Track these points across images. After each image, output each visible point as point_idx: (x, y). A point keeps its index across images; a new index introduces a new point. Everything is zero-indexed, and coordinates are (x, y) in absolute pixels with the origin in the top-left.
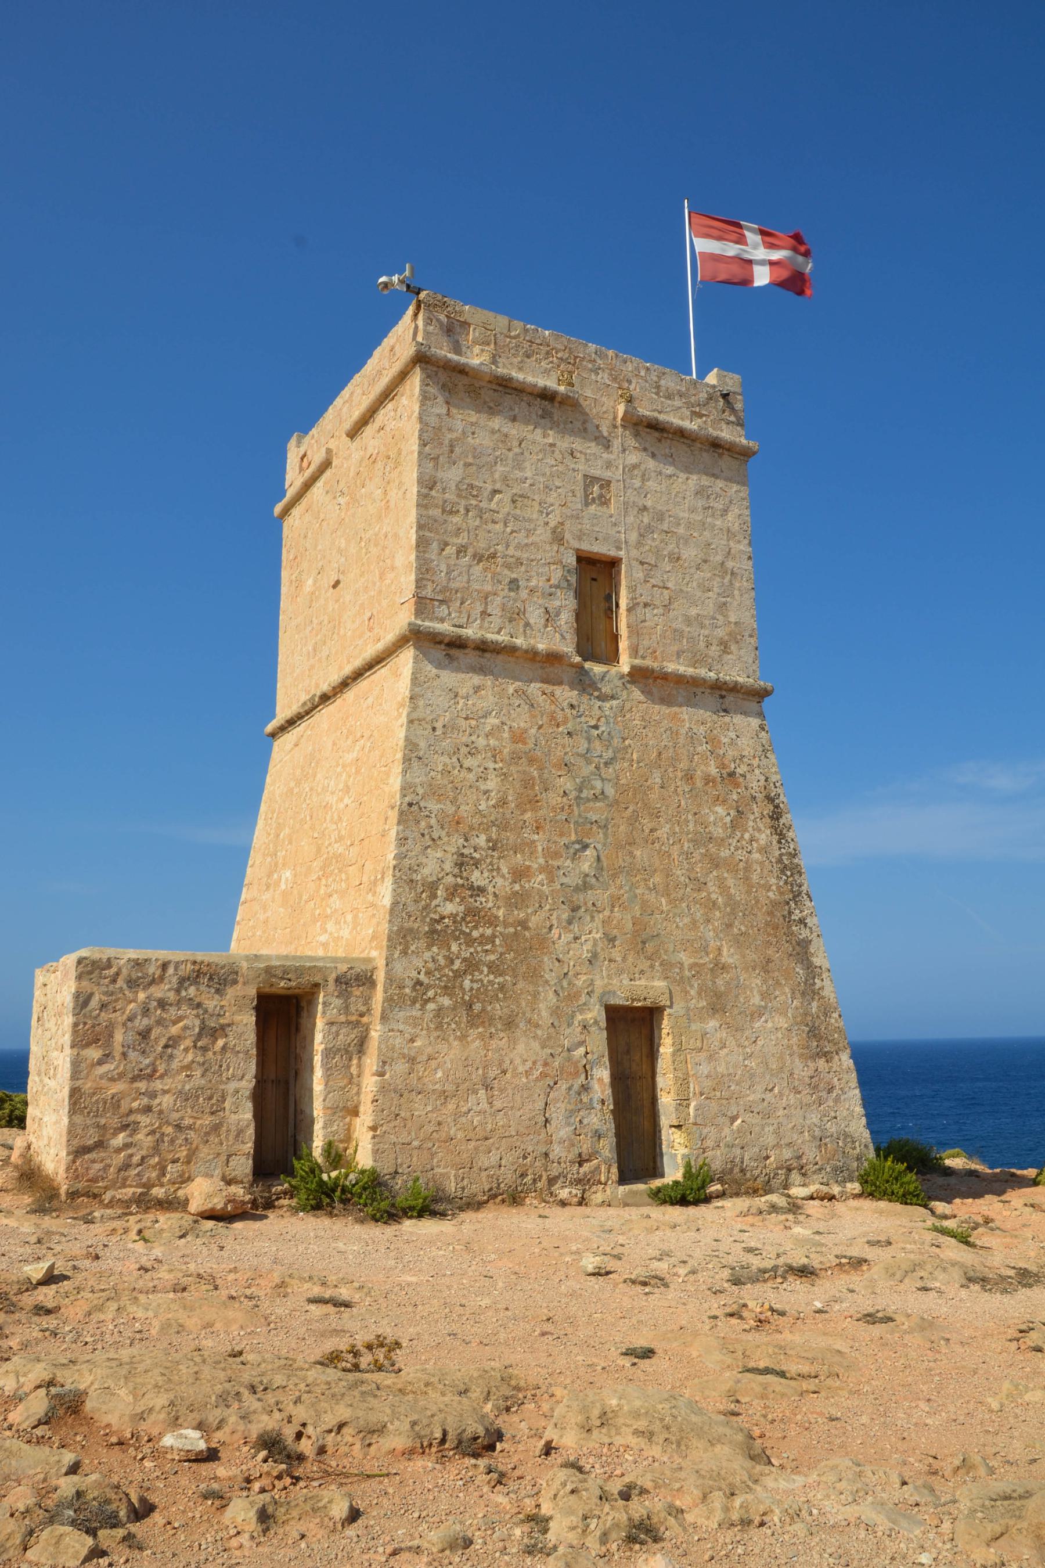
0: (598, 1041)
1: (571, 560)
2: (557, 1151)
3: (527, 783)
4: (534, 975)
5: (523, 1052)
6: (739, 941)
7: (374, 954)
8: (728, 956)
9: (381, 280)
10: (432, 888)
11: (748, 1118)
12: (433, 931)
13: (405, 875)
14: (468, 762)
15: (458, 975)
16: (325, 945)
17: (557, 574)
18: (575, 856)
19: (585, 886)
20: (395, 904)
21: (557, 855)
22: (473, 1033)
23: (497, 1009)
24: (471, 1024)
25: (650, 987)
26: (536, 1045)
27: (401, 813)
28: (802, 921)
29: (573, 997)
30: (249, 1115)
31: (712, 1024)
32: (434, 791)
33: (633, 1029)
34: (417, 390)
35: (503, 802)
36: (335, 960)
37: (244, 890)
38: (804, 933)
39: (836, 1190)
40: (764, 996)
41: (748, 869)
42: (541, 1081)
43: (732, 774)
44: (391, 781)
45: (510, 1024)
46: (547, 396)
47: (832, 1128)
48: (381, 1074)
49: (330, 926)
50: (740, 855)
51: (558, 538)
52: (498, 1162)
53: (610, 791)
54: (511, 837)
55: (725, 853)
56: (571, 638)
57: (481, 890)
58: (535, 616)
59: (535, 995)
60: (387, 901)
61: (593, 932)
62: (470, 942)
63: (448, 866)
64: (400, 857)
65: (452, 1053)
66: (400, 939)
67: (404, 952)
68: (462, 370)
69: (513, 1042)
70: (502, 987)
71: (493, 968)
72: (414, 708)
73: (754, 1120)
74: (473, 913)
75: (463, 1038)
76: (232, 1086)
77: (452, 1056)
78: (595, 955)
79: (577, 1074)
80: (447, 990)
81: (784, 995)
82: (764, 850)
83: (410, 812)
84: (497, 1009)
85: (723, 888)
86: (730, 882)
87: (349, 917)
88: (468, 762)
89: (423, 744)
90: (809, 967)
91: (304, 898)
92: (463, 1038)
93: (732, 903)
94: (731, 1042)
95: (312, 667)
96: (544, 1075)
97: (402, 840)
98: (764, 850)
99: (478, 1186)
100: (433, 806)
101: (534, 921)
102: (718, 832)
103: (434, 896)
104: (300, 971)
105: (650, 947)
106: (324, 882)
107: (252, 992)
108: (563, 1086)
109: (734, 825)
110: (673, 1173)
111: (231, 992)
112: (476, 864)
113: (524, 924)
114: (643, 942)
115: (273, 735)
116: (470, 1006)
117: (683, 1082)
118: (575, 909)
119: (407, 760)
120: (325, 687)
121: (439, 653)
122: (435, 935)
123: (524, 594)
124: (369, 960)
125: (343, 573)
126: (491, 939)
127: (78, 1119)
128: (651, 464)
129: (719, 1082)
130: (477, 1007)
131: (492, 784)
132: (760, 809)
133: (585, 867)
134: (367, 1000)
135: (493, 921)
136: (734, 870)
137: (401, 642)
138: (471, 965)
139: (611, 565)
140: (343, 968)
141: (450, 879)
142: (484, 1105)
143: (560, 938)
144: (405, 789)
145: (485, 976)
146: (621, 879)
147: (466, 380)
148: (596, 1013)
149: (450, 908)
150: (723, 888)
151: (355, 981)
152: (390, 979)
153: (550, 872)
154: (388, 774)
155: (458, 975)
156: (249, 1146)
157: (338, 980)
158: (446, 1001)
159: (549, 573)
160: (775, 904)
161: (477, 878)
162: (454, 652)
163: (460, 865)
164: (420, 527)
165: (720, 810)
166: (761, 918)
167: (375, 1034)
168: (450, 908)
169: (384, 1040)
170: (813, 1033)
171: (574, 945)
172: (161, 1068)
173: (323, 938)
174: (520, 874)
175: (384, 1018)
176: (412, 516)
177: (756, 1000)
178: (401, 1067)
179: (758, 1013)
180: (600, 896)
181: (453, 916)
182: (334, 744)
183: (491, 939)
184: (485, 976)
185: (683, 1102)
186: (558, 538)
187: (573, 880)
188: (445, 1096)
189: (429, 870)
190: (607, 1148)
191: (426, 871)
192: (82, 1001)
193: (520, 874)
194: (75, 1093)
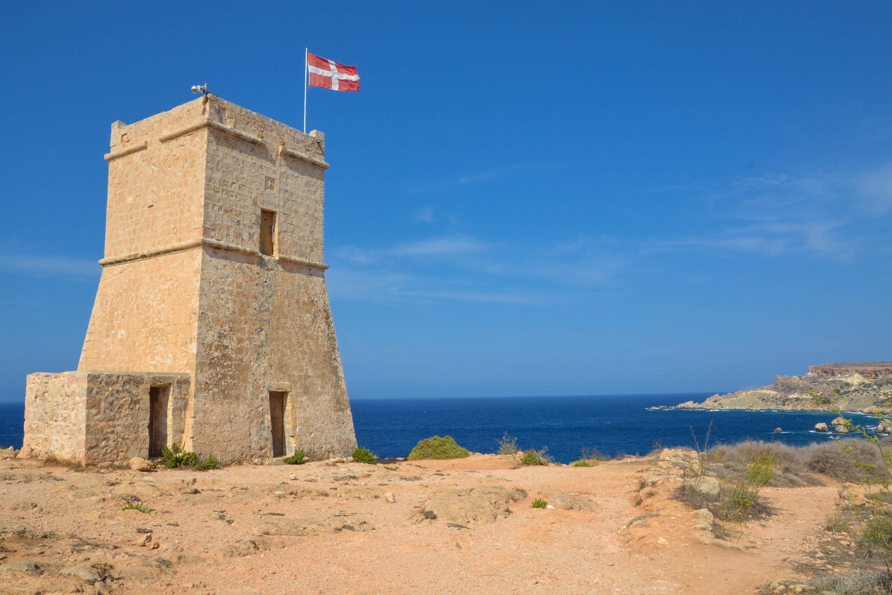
0: (267, 405)
1: (259, 212)
2: (254, 445)
3: (242, 305)
4: (245, 380)
5: (242, 409)
6: (314, 367)
7: (188, 371)
8: (311, 373)
9: (194, 87)
10: (210, 346)
11: (316, 433)
12: (211, 363)
13: (201, 342)
14: (222, 296)
15: (220, 380)
16: (155, 366)
17: (254, 219)
18: (258, 334)
19: (262, 346)
20: (198, 352)
21: (252, 333)
22: (225, 402)
23: (233, 393)
24: (225, 398)
25: (283, 384)
26: (246, 406)
27: (199, 317)
28: (335, 359)
29: (258, 388)
30: (147, 434)
31: (305, 398)
32: (211, 308)
33: (278, 399)
34: (206, 138)
35: (234, 312)
36: (176, 374)
37: (87, 336)
38: (336, 364)
39: (345, 459)
40: (322, 387)
41: (317, 339)
42: (246, 419)
43: (312, 301)
44: (193, 302)
45: (237, 398)
46: (254, 142)
47: (344, 437)
48: (194, 417)
49: (157, 358)
50: (315, 333)
51: (255, 204)
52: (234, 449)
53: (271, 308)
54: (237, 326)
55: (309, 333)
56: (258, 245)
57: (227, 347)
58: (245, 236)
59: (246, 387)
60: (195, 351)
61: (265, 363)
62: (223, 367)
63: (215, 338)
64: (199, 334)
65: (218, 409)
66: (200, 366)
67: (201, 371)
68: (223, 131)
69: (239, 405)
70: (234, 384)
71: (232, 377)
72: (203, 274)
73: (318, 434)
74: (224, 356)
75: (222, 404)
76: (142, 423)
77: (218, 410)
78: (266, 372)
79: (259, 417)
80: (216, 385)
81: (328, 387)
82: (323, 331)
83: (202, 317)
84: (233, 393)
85: (309, 346)
86: (311, 344)
87: (170, 356)
88: (222, 296)
89: (206, 289)
90: (337, 376)
91: (137, 344)
92: (222, 404)
93: (312, 352)
94: (311, 405)
95: (132, 239)
96: (249, 417)
97: (200, 327)
98: (323, 331)
99: (227, 459)
100: (210, 314)
101: (245, 359)
102: (307, 324)
103: (211, 349)
104: (165, 378)
105: (284, 369)
106: (150, 338)
107: (148, 387)
108: (255, 421)
109: (313, 321)
110: (290, 454)
111: (141, 387)
112: (225, 337)
113: (241, 360)
114: (282, 367)
115: (104, 265)
116: (224, 392)
117: (295, 419)
118: (259, 354)
119: (201, 295)
120: (146, 252)
121: (211, 251)
122: (212, 365)
123: (242, 226)
124: (187, 374)
126: (231, 366)
127: (89, 436)
128: (290, 172)
129: (307, 420)
130: (226, 392)
131: (230, 305)
132: (322, 315)
133: (262, 338)
134: (187, 389)
135: (231, 359)
136: (312, 339)
137: (196, 245)
138: (224, 376)
139: (273, 214)
140: (179, 377)
141: (216, 343)
142: (229, 429)
143: (254, 365)
144: (201, 307)
145: (229, 380)
146: (274, 343)
147: (224, 134)
148: (266, 394)
149: (216, 354)
150: (309, 346)
151: (184, 382)
152: (197, 382)
153: (250, 339)
154: (191, 300)
155: (220, 380)
156: (147, 445)
157: (178, 382)
158: (216, 390)
159: (251, 217)
160: (326, 352)
161: (226, 342)
162: (217, 251)
163: (219, 337)
164: (206, 198)
165: (308, 315)
166: (321, 358)
167: (192, 402)
168: (216, 354)
169: (195, 405)
170: (338, 402)
171: (259, 368)
172: (117, 417)
173: (153, 362)
174: (240, 341)
175: (195, 396)
176: (202, 192)
177: (319, 389)
178: (201, 415)
179: (320, 394)
180: (267, 349)
181: (218, 357)
182: (151, 278)
183: (231, 366)
184: (229, 380)
185: (295, 427)
186: (255, 204)
187: (258, 343)
188: (216, 425)
189: (209, 339)
190: (270, 444)
191: (208, 340)
192: (90, 391)
193: (240, 341)
194: (88, 426)
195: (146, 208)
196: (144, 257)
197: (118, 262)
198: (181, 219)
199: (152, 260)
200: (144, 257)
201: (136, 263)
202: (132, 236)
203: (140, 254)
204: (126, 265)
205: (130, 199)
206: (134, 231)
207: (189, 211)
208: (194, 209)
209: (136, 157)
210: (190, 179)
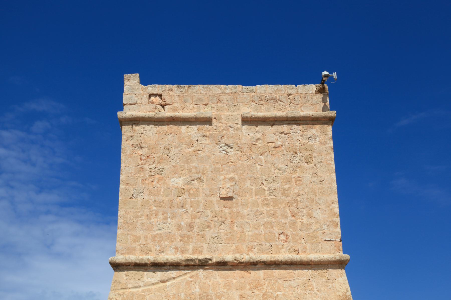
34: (330, 134)
125: (237, 194)
137: (339, 264)
195: (216, 198)
196: (222, 265)
197: (157, 266)
198: (293, 224)
199: (238, 273)
200: (222, 265)
201: (201, 272)
202: (184, 232)
203: (214, 260)
204: (174, 273)
205: (178, 182)
206: (191, 226)
207: (310, 216)
208: (318, 214)
209: (194, 130)
210: (307, 176)
